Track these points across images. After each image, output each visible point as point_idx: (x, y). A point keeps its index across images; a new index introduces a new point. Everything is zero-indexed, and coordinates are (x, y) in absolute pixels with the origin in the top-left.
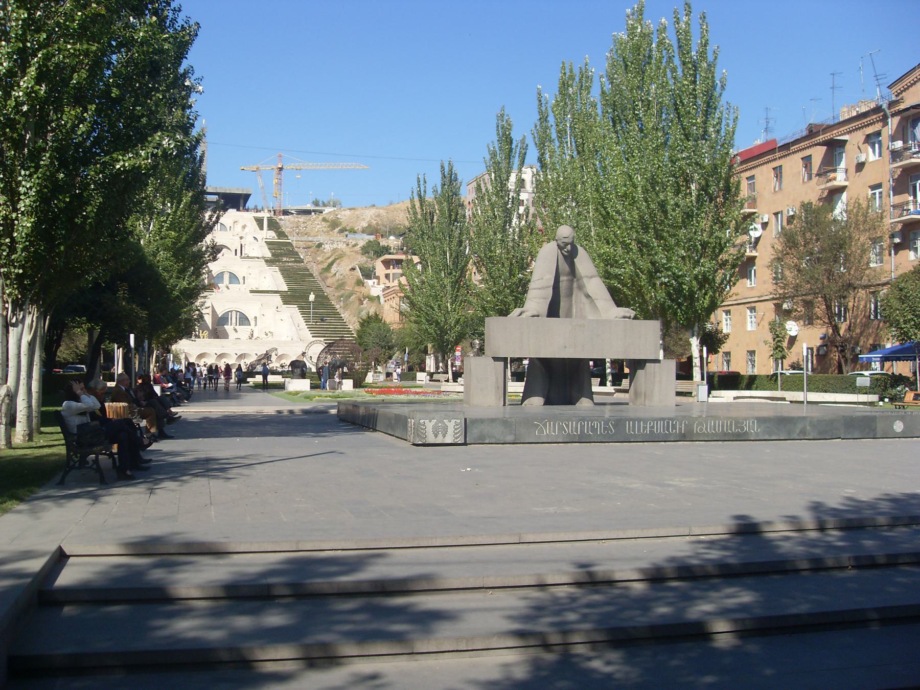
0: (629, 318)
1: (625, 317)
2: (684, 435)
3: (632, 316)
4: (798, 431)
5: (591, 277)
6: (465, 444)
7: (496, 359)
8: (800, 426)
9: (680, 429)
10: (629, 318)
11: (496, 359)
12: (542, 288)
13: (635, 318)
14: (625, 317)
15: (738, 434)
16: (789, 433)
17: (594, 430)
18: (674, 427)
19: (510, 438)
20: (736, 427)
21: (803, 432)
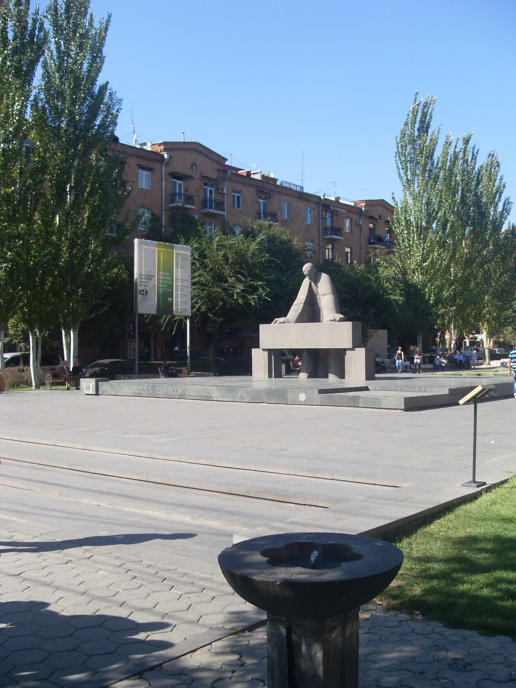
0: (334, 320)
1: (331, 321)
2: (182, 396)
3: (338, 319)
4: (239, 396)
5: (325, 295)
6: (97, 394)
7: (264, 350)
8: (240, 394)
9: (180, 392)
10: (334, 320)
11: (264, 350)
12: (297, 305)
13: (341, 320)
14: (331, 321)
15: (207, 397)
16: (234, 398)
17: (143, 390)
18: (177, 391)
19: (113, 393)
20: (206, 392)
21: (242, 397)
